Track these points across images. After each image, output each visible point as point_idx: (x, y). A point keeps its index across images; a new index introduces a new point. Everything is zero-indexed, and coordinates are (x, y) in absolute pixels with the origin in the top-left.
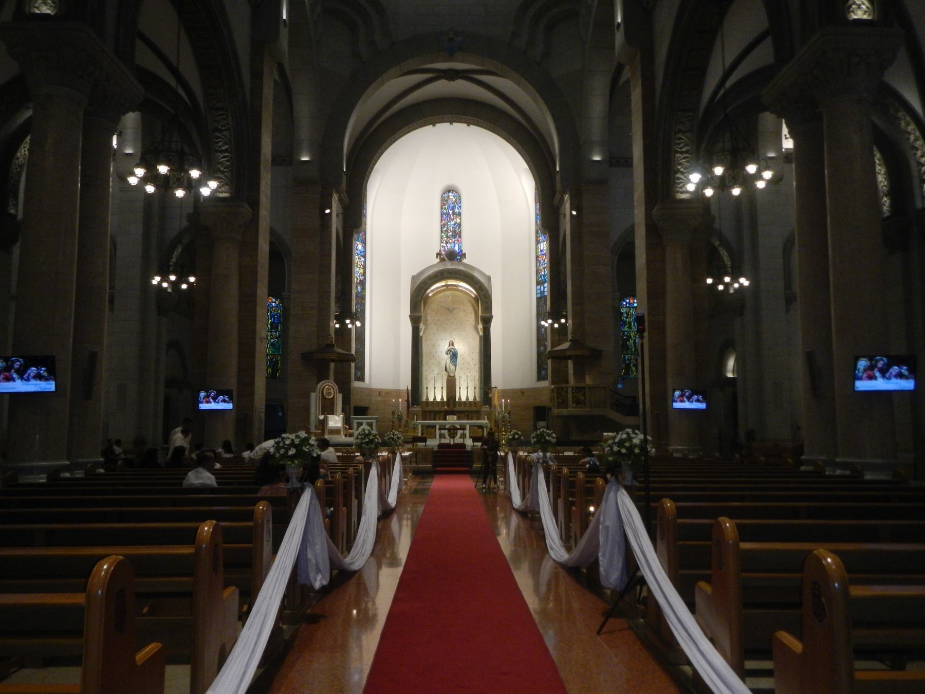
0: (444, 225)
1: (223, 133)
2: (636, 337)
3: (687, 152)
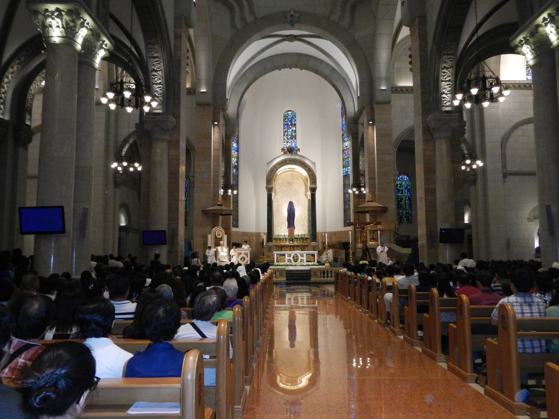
0: (286, 131)
1: (158, 72)
2: (406, 199)
3: (449, 81)
